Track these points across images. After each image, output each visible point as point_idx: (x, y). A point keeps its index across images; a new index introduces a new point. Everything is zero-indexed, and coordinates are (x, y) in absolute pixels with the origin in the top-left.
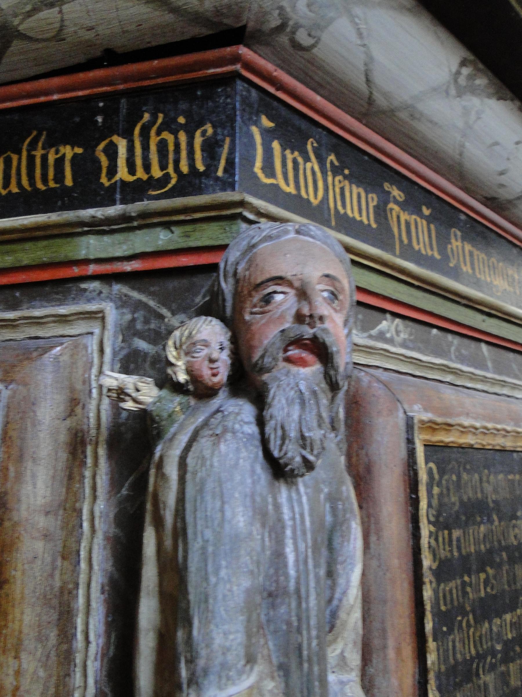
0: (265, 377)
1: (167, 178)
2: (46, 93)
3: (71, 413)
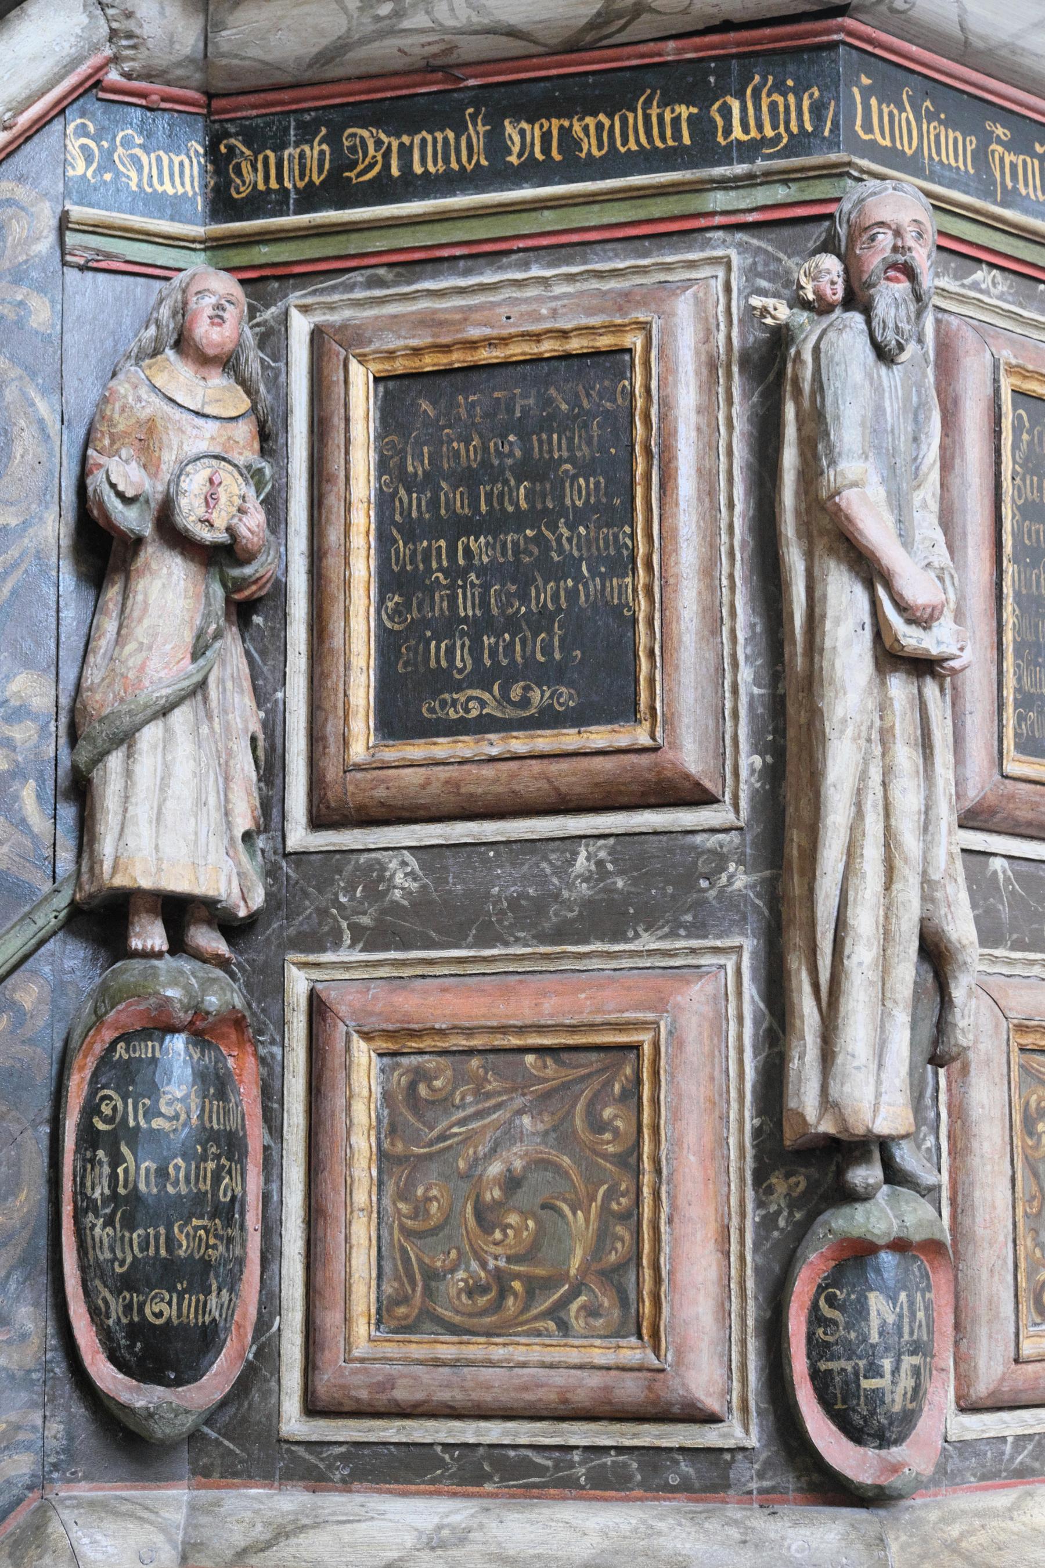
0: (872, 291)
1: (778, 137)
3: (707, 341)
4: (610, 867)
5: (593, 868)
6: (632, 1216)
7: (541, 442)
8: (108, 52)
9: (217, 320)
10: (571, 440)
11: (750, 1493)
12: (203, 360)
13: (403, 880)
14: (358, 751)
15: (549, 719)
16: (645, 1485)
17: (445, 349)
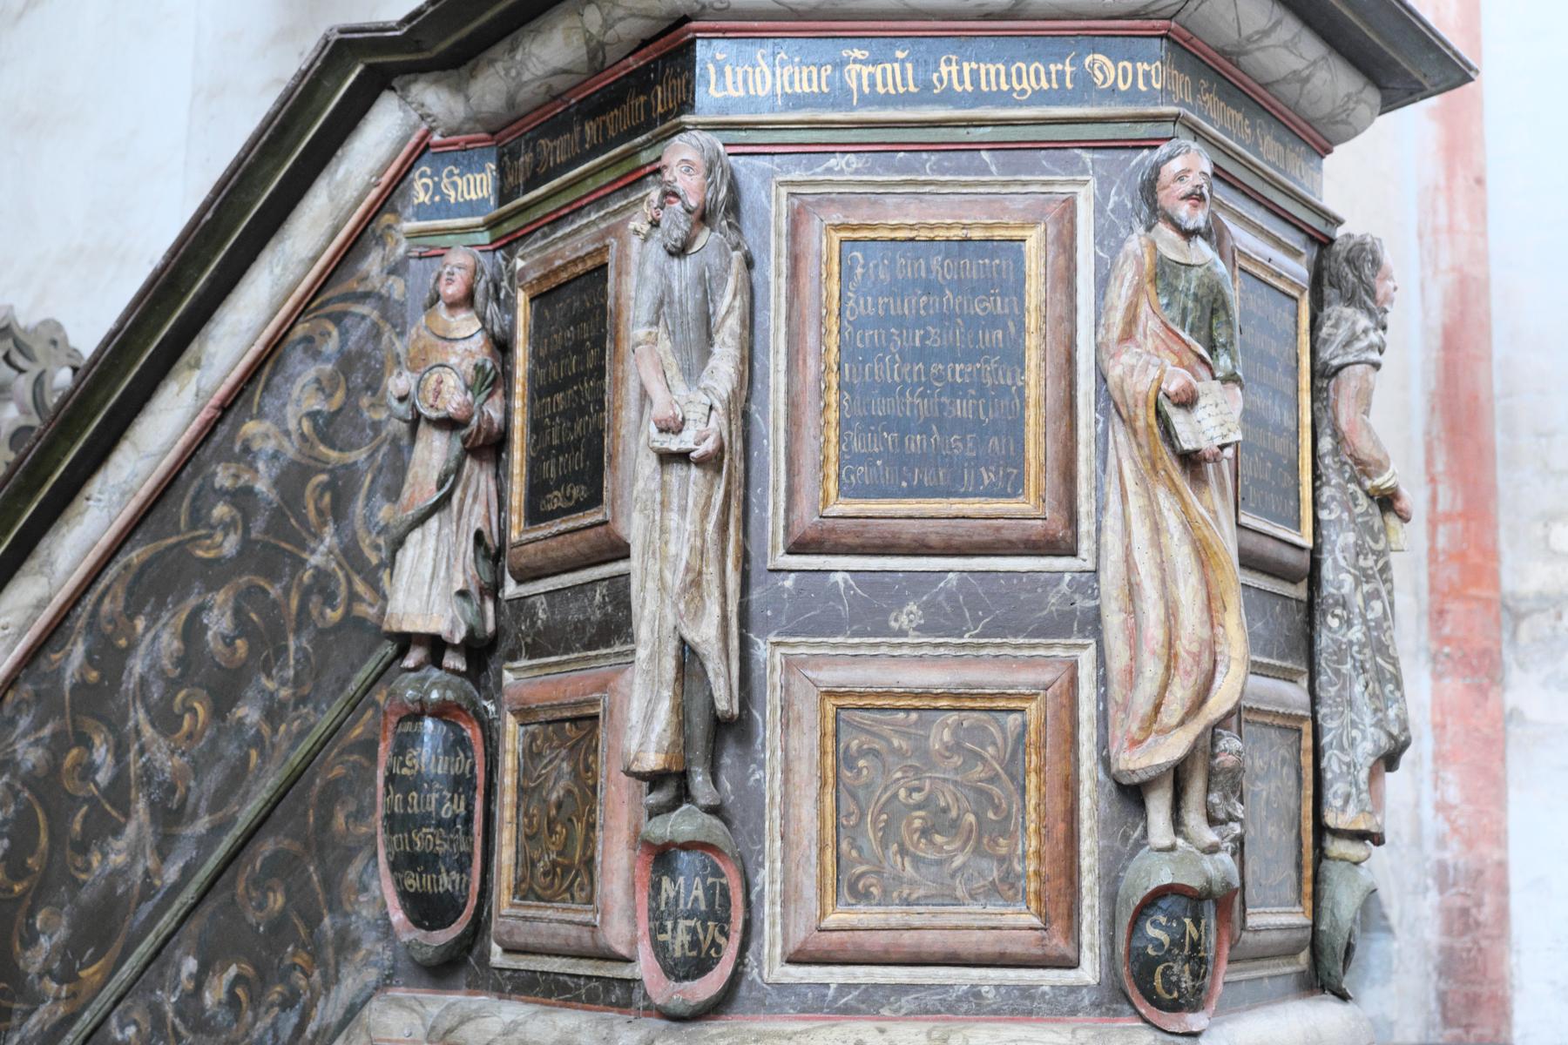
8: (424, 127)
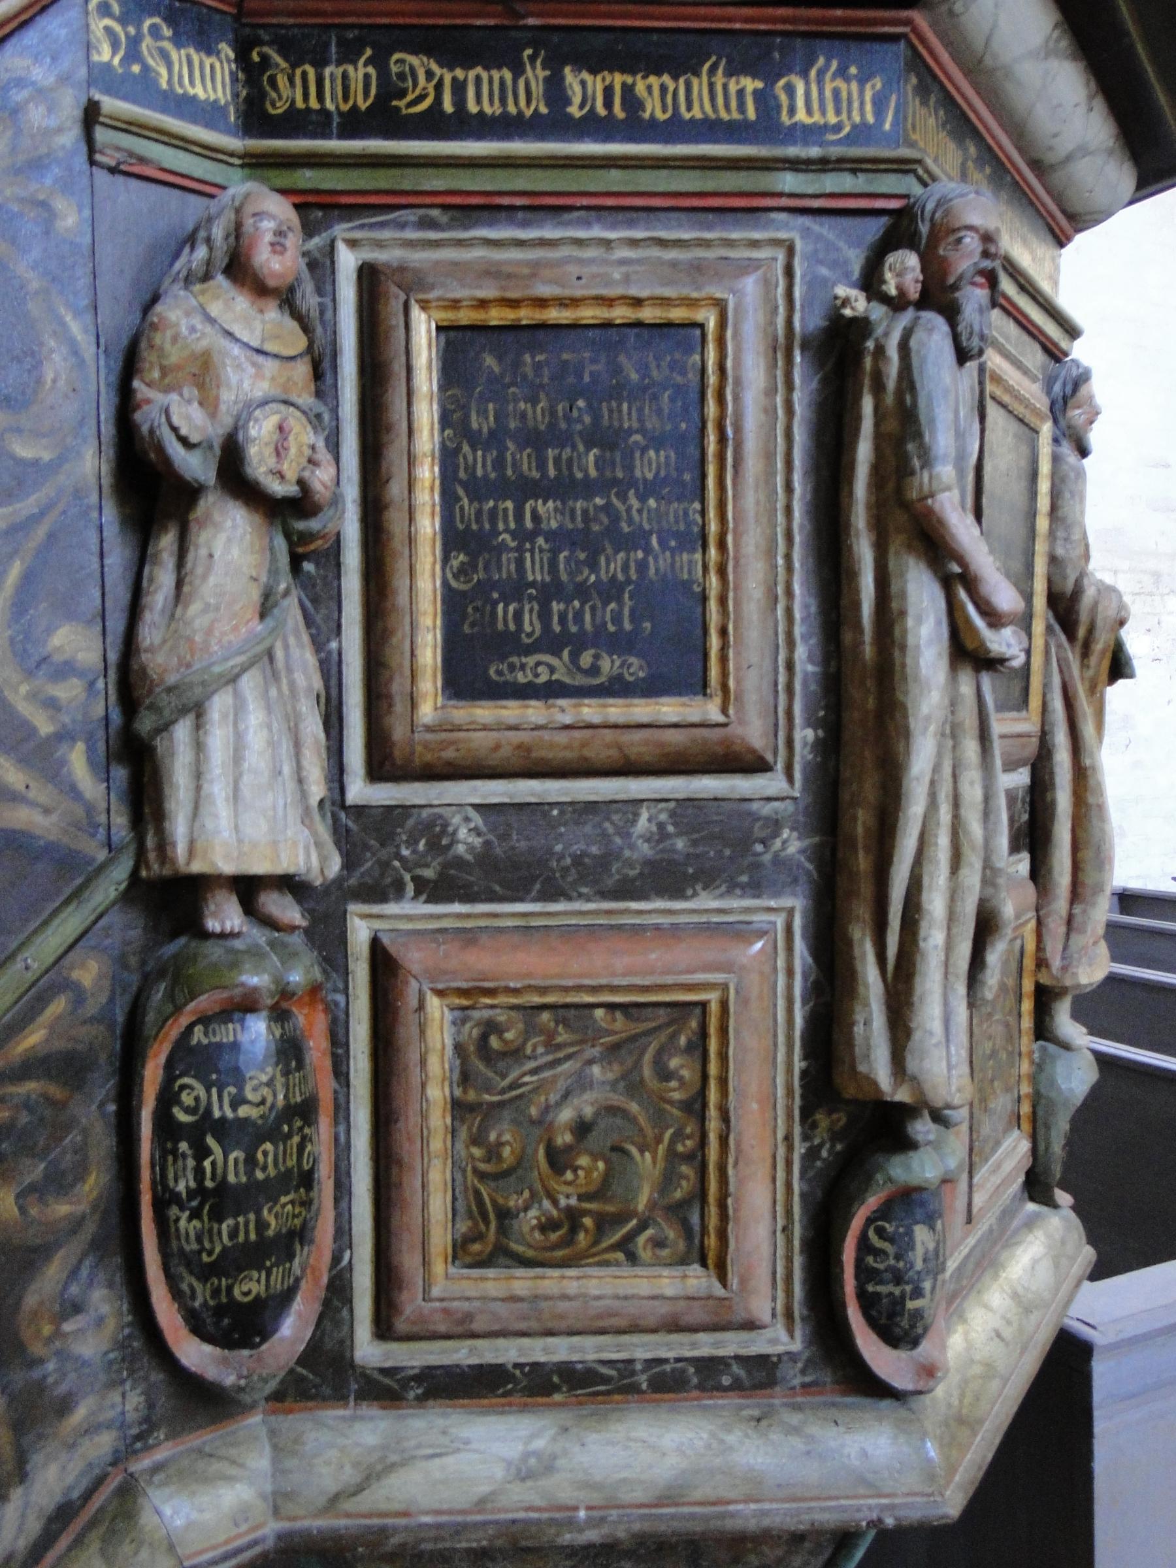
2: (730, 20)
4: (671, 829)
5: (654, 829)
6: (698, 1157)
7: (611, 411)
9: (278, 248)
10: (640, 410)
11: (793, 1388)
12: (260, 289)
13: (466, 838)
14: (427, 712)
15: (618, 688)
16: (701, 1387)
17: (514, 304)
